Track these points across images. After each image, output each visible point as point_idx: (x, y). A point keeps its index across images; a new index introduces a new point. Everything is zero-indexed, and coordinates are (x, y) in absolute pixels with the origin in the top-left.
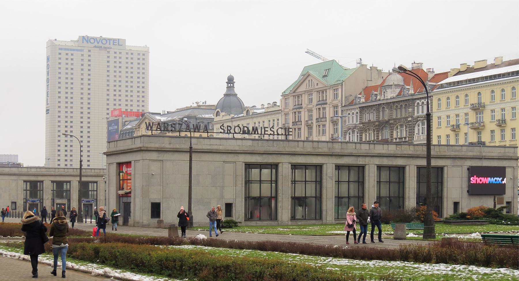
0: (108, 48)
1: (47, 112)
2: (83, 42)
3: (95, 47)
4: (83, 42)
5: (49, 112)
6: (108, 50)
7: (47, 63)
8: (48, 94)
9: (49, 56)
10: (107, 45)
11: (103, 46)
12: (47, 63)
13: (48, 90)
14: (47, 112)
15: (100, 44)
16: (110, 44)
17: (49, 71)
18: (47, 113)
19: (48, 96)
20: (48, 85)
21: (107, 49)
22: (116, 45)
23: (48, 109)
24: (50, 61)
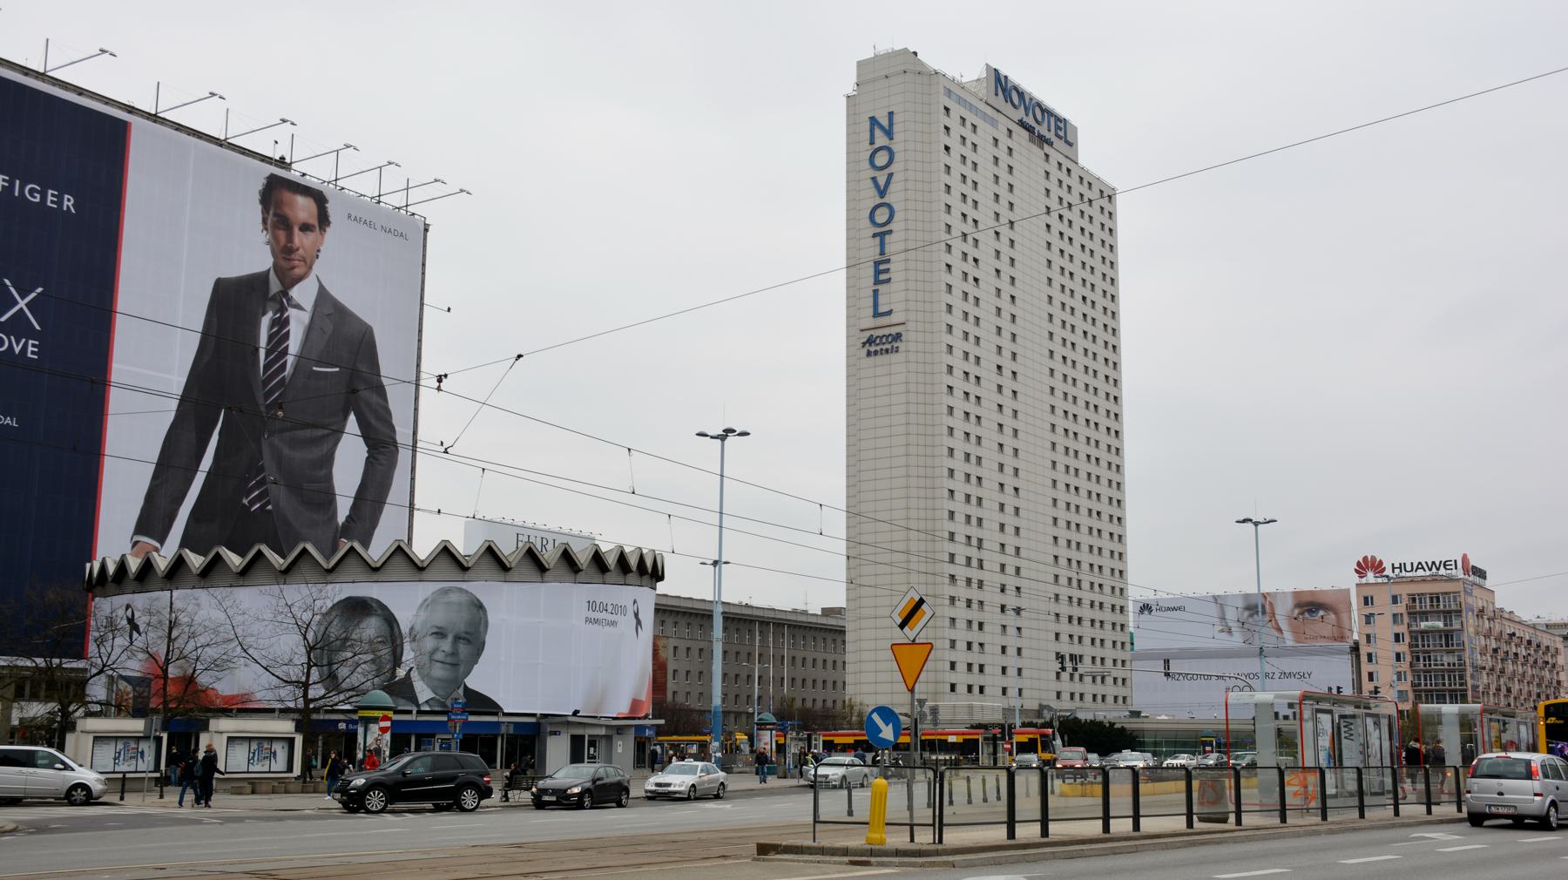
0: (1047, 143)
1: (873, 349)
2: (997, 95)
3: (1022, 124)
4: (997, 95)
5: (895, 345)
6: (1047, 148)
7: (872, 143)
8: (878, 272)
9: (891, 114)
10: (1042, 130)
11: (1037, 128)
12: (872, 143)
13: (882, 253)
14: (873, 349)
15: (1030, 121)
16: (1049, 130)
17: (891, 175)
18: (869, 354)
19: (877, 282)
20: (881, 236)
21: (1045, 146)
22: (1060, 137)
23: (877, 333)
24: (895, 136)
